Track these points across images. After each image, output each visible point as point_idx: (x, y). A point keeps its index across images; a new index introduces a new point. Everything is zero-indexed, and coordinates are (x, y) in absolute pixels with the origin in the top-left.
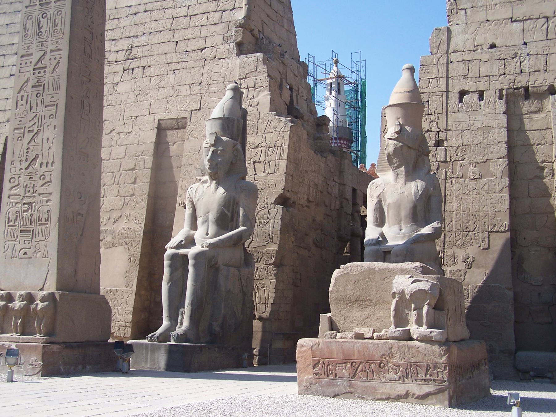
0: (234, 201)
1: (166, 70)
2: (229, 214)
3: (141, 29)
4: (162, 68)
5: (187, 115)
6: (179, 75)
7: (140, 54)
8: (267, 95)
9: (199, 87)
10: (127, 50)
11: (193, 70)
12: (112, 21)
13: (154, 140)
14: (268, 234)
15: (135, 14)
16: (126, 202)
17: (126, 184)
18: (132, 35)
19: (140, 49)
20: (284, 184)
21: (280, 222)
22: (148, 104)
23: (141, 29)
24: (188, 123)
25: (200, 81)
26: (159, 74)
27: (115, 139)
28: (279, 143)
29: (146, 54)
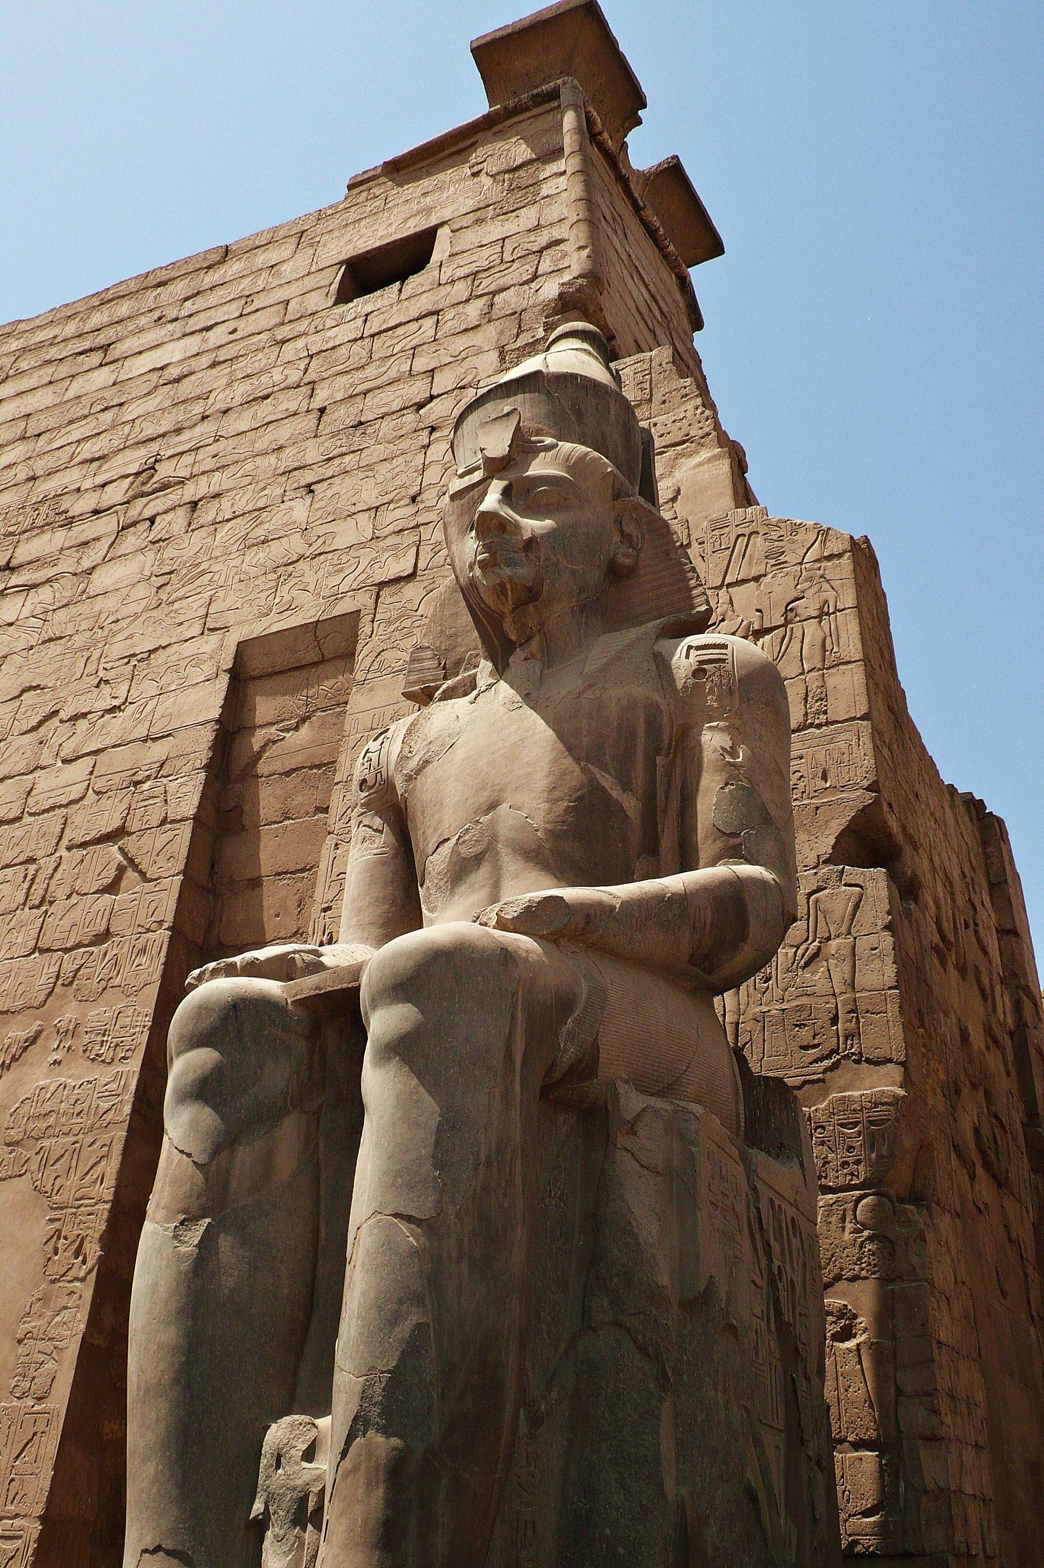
0: (653, 726)
1: (279, 491)
2: (631, 804)
3: (198, 408)
4: (264, 488)
5: (364, 600)
6: (329, 493)
7: (184, 473)
8: (716, 458)
9: (412, 509)
10: (138, 474)
11: (383, 469)
12: (101, 416)
13: (215, 713)
14: (825, 1018)
15: (177, 380)
16: (68, 968)
17: (75, 899)
18: (162, 431)
19: (187, 459)
20: (869, 762)
21: (887, 940)
22: (202, 601)
23: (198, 408)
24: (367, 630)
25: (413, 491)
26: (250, 507)
27: (55, 741)
28: (808, 606)
29: (209, 464)
